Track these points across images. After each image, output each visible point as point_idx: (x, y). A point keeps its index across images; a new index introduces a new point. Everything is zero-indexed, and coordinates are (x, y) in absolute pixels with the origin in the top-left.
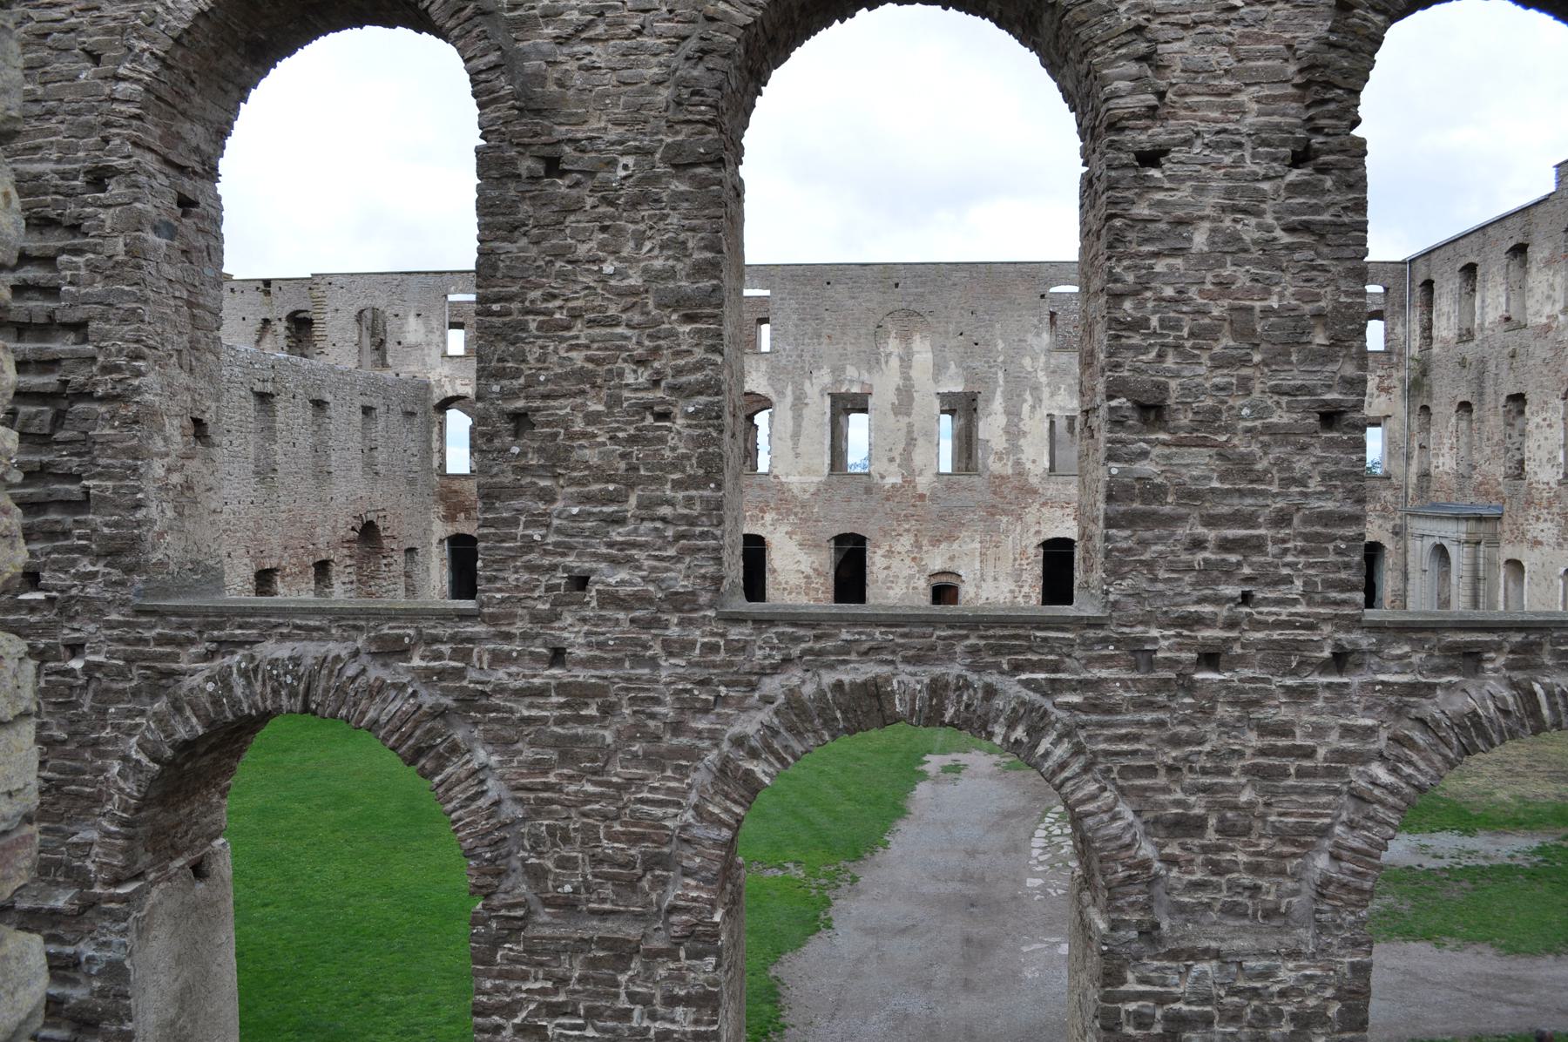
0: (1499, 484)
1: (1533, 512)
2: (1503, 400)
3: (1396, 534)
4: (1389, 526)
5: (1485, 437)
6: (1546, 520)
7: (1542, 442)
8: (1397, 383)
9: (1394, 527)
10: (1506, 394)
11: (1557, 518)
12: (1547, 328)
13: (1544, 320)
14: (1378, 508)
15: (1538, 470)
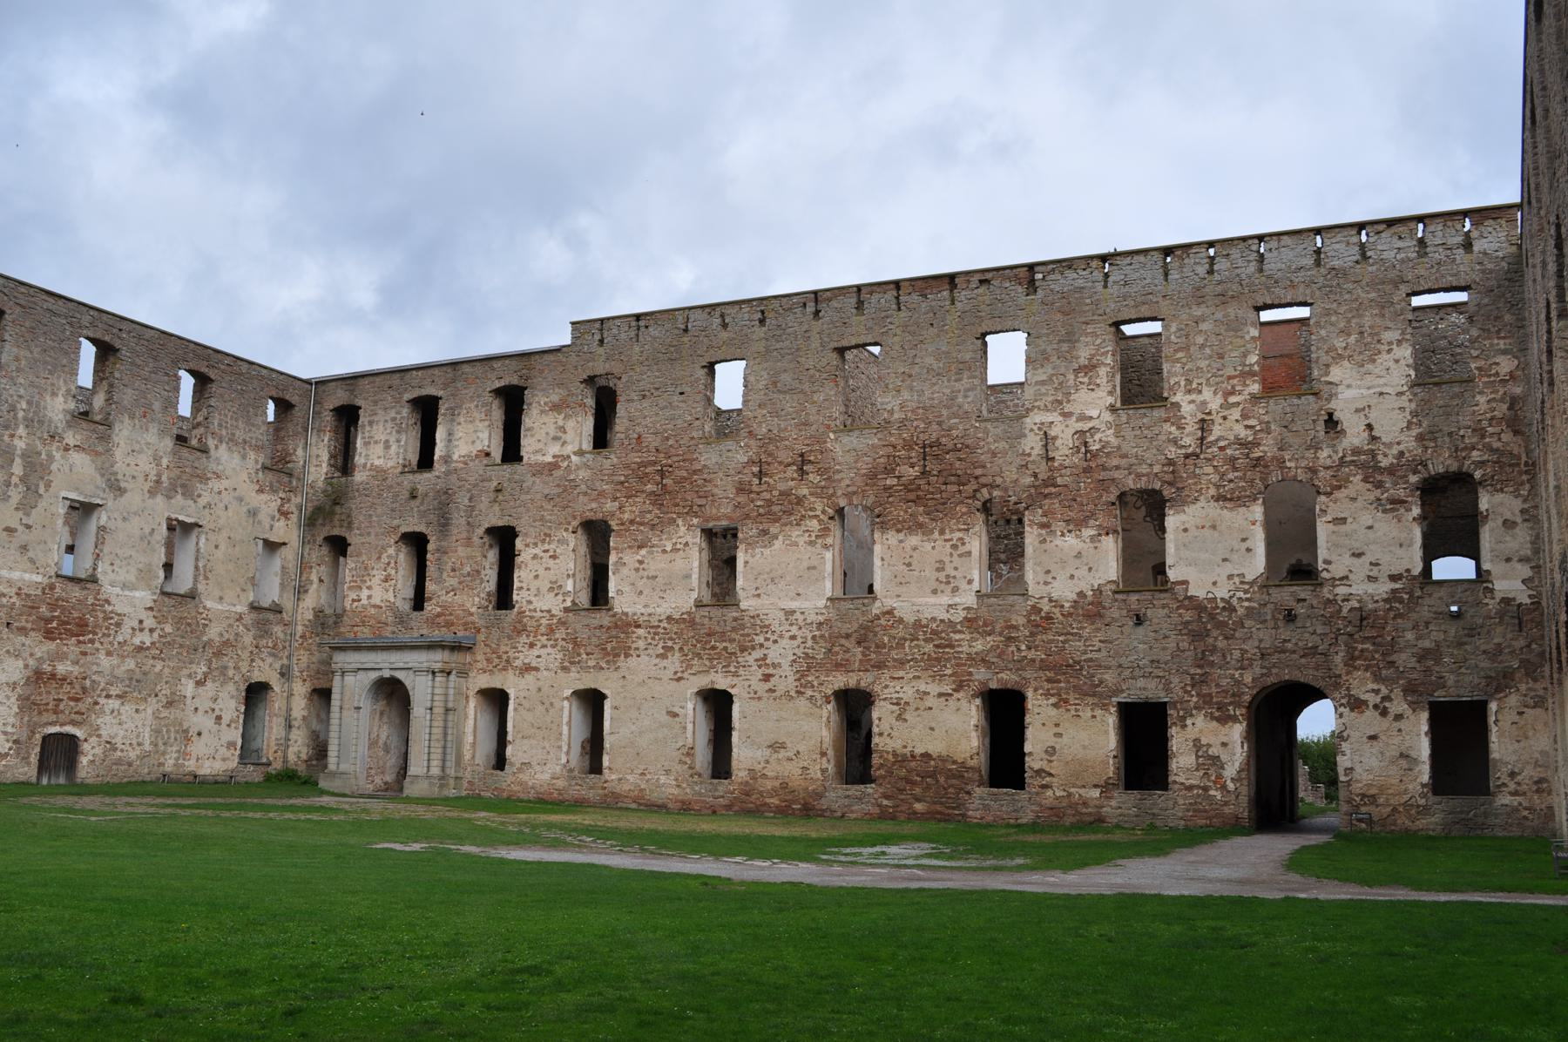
0: (472, 614)
1: (523, 639)
2: (481, 531)
3: (282, 675)
4: (277, 665)
5: (448, 567)
6: (544, 646)
7: (541, 572)
8: (294, 509)
9: (282, 666)
10: (487, 526)
11: (561, 643)
12: (554, 466)
13: (549, 459)
14: (270, 645)
15: (533, 599)
